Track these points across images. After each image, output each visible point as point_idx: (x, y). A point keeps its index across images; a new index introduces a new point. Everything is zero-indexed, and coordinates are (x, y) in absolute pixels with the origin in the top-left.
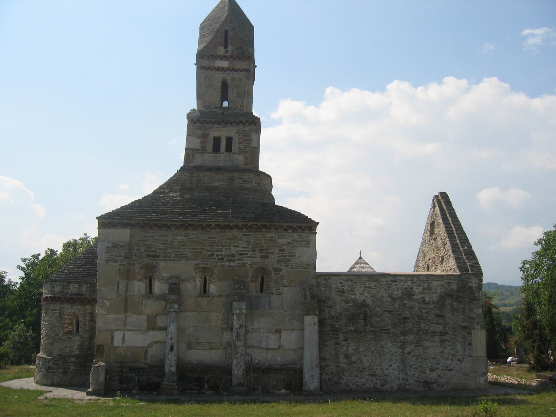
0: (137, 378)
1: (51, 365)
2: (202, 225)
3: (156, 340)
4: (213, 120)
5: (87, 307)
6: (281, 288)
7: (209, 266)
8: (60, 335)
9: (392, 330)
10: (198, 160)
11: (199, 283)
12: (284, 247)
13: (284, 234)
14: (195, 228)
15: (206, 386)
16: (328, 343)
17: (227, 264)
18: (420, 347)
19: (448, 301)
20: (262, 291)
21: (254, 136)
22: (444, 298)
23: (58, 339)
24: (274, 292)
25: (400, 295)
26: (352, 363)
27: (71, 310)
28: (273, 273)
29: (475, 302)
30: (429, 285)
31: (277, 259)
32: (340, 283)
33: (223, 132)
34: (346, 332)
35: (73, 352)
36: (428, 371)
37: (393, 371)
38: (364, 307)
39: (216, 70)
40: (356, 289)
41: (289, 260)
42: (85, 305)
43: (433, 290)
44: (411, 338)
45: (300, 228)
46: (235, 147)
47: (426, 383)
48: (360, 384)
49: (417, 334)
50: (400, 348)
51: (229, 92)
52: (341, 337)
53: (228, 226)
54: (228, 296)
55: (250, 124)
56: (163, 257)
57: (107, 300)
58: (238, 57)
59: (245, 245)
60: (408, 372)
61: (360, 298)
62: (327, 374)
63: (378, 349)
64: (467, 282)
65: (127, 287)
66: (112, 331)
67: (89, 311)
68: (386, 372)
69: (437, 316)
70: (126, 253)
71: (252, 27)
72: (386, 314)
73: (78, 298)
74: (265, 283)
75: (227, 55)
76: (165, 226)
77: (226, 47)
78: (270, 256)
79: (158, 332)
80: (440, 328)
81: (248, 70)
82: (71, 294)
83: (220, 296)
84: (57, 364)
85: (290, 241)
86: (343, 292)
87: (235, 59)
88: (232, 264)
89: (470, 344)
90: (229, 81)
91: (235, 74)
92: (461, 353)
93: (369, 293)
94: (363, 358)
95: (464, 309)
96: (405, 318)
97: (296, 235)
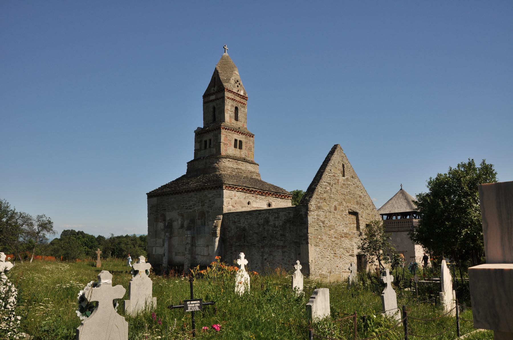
12: (211, 199)
41: (212, 206)
44: (267, 250)
50: (261, 256)
52: (233, 249)
61: (242, 225)
69: (281, 235)
72: (255, 235)
78: (206, 204)
80: (281, 244)
86: (235, 222)
88: (191, 211)
89: (299, 254)
91: (218, 102)
93: (247, 222)
96: (264, 237)
97: (215, 191)
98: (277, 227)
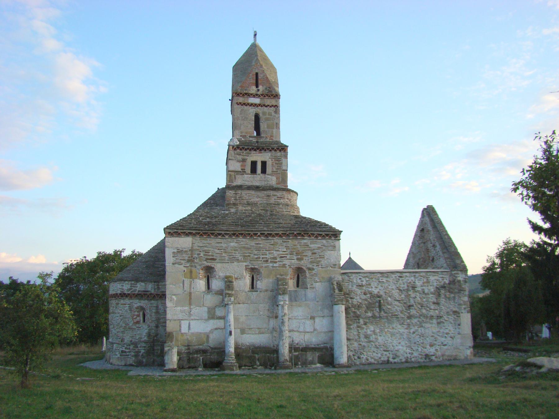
0: (201, 358)
1: (124, 349)
2: (249, 234)
3: (215, 327)
4: (250, 147)
5: (153, 302)
6: (314, 284)
7: (256, 267)
8: (130, 325)
9: (401, 315)
10: (239, 181)
11: (248, 280)
12: (315, 251)
13: (315, 240)
14: (244, 236)
15: (258, 363)
16: (351, 327)
17: (271, 265)
18: (422, 329)
19: (443, 292)
20: (298, 286)
21: (283, 160)
22: (439, 289)
23: (129, 328)
24: (309, 287)
25: (406, 288)
26: (370, 342)
27: (139, 304)
28: (307, 272)
29: (462, 292)
30: (428, 280)
31: (310, 260)
32: (360, 279)
33: (258, 157)
34: (366, 318)
35: (141, 338)
36: (428, 347)
37: (401, 347)
38: (379, 297)
39: (250, 106)
40: (372, 284)
41: (319, 261)
42: (151, 300)
43: (431, 284)
44: (415, 321)
45: (327, 235)
46: (269, 169)
47: (427, 356)
48: (376, 358)
49: (420, 318)
50: (407, 329)
51: (261, 124)
52: (361, 321)
53: (271, 234)
54: (272, 291)
55: (280, 151)
56: (219, 260)
57: (175, 295)
58: (267, 95)
59: (285, 250)
60: (413, 347)
61: (375, 291)
62: (351, 351)
63: (390, 330)
64: (456, 277)
65: (190, 285)
66: (180, 320)
67: (155, 305)
68: (396, 348)
69: (434, 303)
70: (189, 257)
71: (276, 69)
72: (397, 303)
73: (144, 294)
74: (300, 280)
75: (259, 93)
76: (220, 234)
77: (257, 86)
78: (304, 258)
79: (218, 320)
81: (276, 106)
82: (139, 291)
83: (266, 291)
84: (129, 349)
85: (319, 246)
86: (361, 286)
87: (265, 96)
88: (275, 265)
89: (459, 325)
90: (261, 115)
91: (265, 109)
92: (452, 332)
94: (379, 338)
95: (454, 297)
96: (410, 306)
97: (324, 241)
98: (428, 294)
